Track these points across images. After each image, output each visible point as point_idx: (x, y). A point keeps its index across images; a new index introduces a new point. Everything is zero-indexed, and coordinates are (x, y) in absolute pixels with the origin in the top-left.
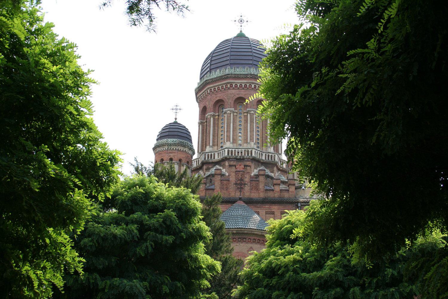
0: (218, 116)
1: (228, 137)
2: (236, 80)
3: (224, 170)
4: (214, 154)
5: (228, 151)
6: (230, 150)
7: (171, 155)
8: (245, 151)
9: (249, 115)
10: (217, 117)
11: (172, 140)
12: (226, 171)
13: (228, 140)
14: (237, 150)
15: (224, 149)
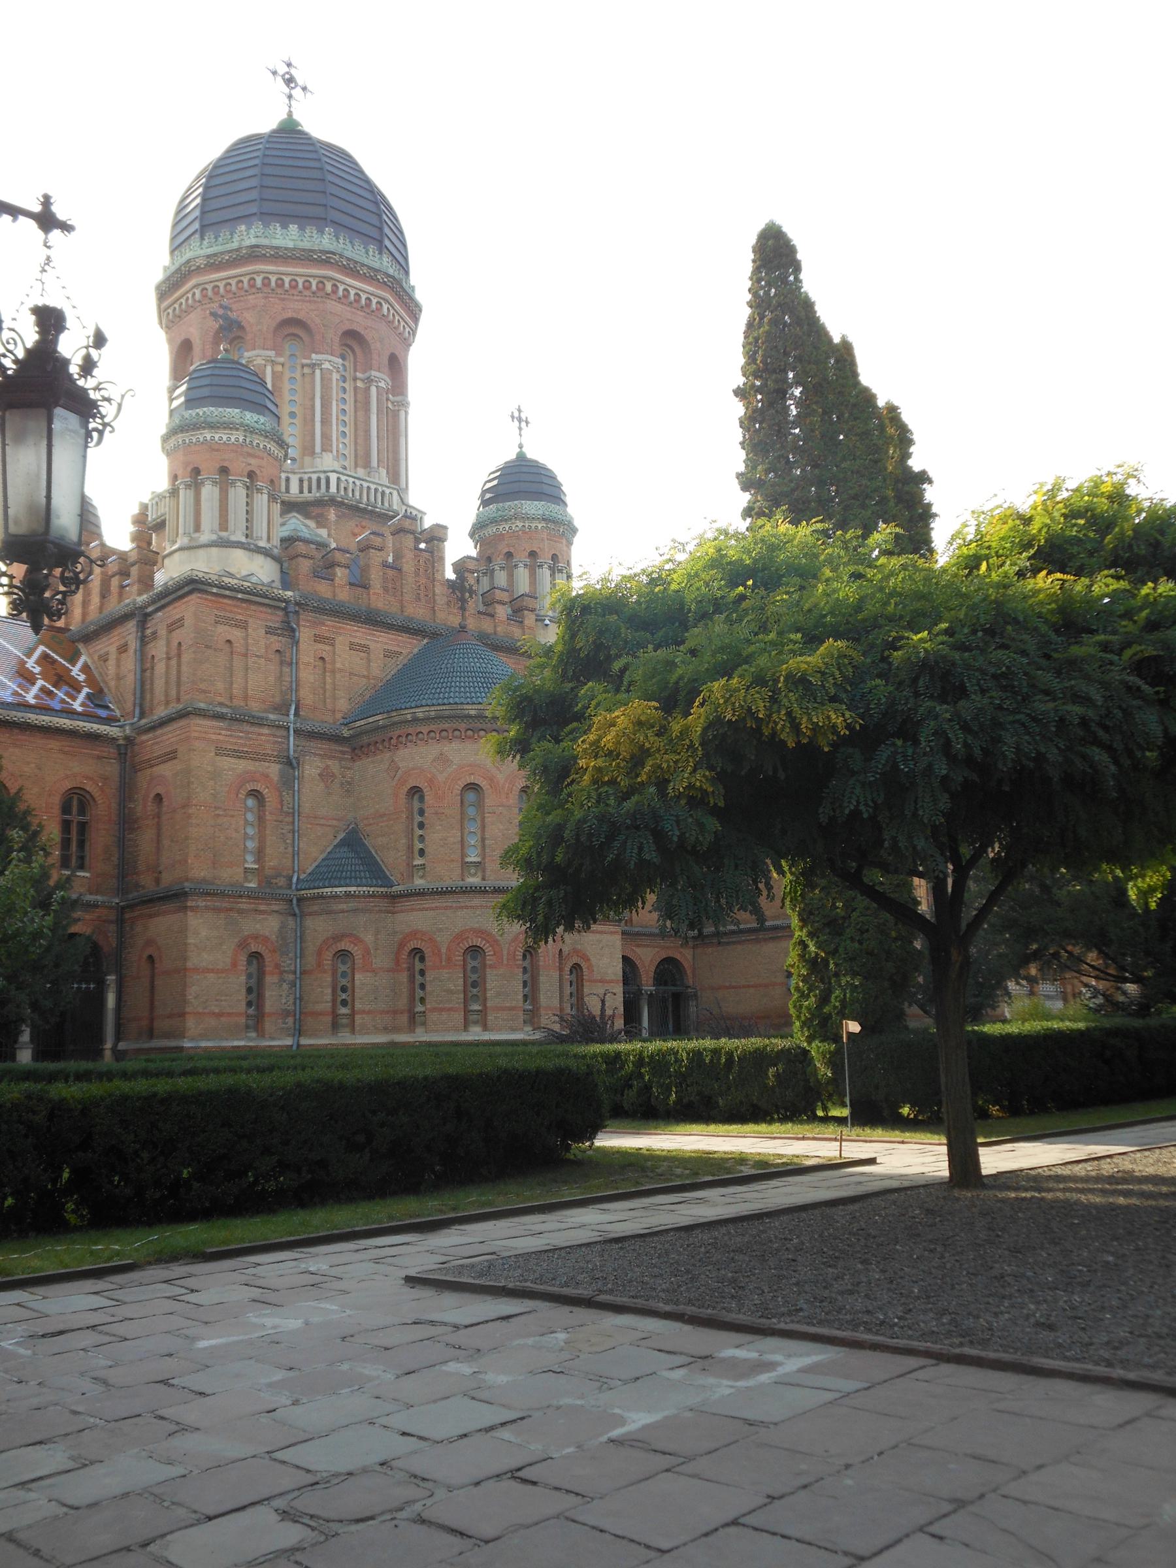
0: (283, 365)
1: (326, 437)
2: (347, 275)
3: (323, 532)
4: (288, 480)
5: (338, 478)
6: (343, 478)
7: (253, 461)
8: (376, 490)
9: (373, 390)
10: (279, 368)
11: (256, 417)
12: (329, 535)
13: (326, 448)
14: (358, 483)
15: (325, 472)
